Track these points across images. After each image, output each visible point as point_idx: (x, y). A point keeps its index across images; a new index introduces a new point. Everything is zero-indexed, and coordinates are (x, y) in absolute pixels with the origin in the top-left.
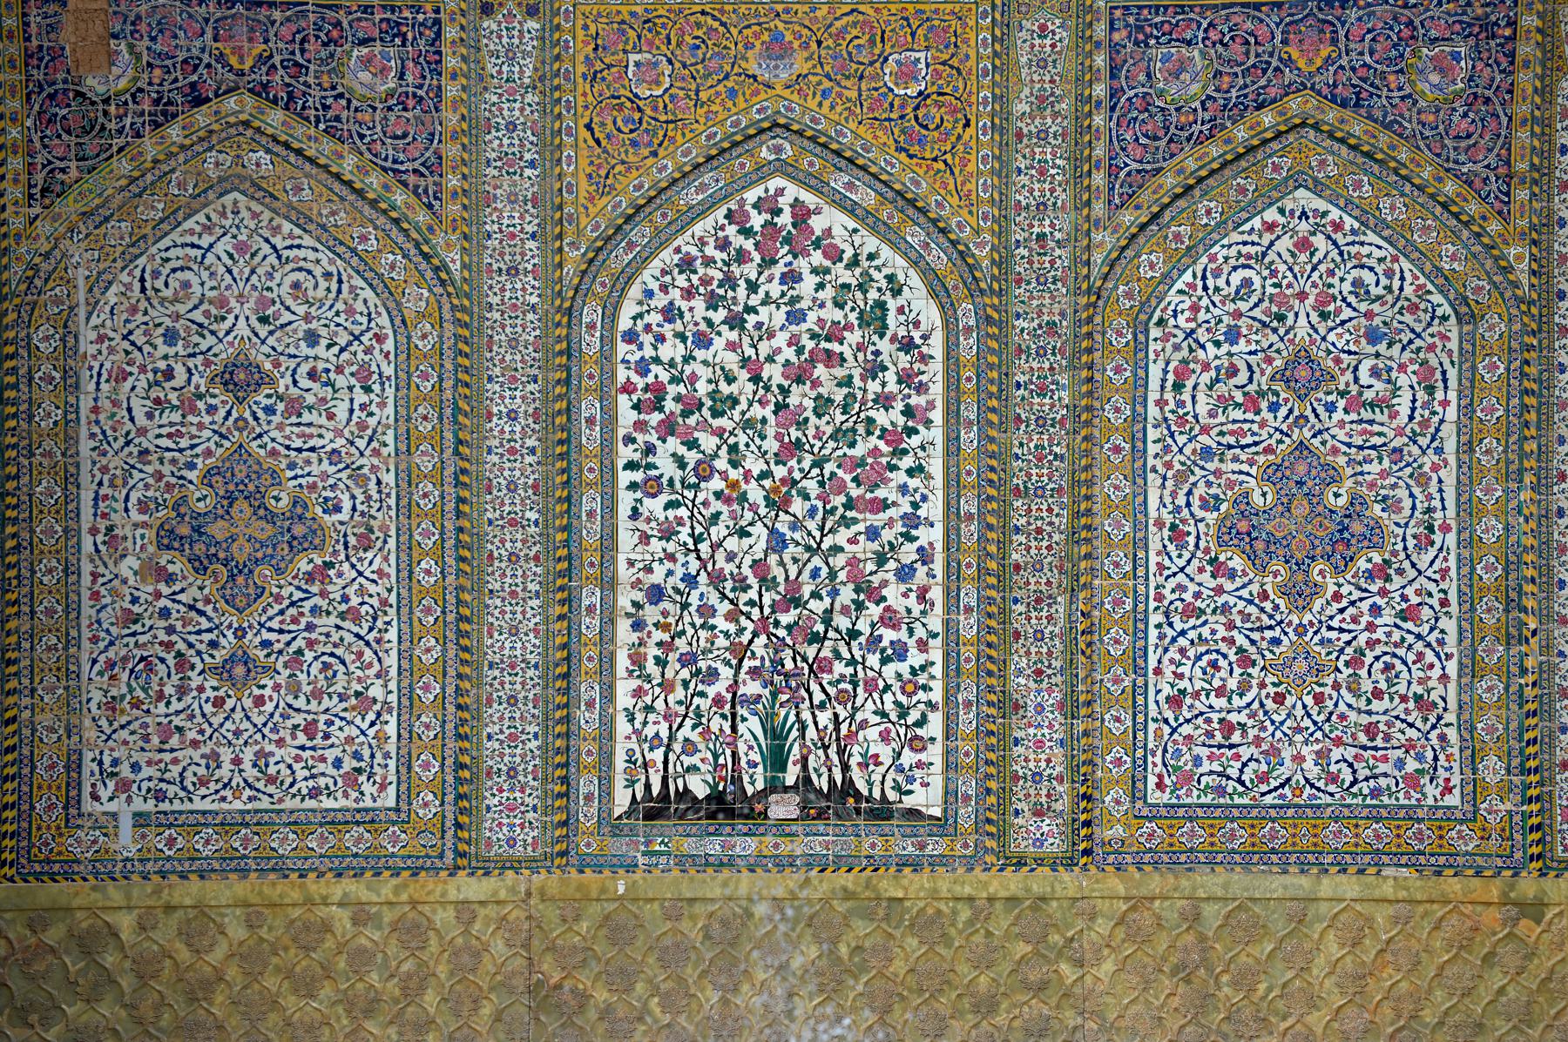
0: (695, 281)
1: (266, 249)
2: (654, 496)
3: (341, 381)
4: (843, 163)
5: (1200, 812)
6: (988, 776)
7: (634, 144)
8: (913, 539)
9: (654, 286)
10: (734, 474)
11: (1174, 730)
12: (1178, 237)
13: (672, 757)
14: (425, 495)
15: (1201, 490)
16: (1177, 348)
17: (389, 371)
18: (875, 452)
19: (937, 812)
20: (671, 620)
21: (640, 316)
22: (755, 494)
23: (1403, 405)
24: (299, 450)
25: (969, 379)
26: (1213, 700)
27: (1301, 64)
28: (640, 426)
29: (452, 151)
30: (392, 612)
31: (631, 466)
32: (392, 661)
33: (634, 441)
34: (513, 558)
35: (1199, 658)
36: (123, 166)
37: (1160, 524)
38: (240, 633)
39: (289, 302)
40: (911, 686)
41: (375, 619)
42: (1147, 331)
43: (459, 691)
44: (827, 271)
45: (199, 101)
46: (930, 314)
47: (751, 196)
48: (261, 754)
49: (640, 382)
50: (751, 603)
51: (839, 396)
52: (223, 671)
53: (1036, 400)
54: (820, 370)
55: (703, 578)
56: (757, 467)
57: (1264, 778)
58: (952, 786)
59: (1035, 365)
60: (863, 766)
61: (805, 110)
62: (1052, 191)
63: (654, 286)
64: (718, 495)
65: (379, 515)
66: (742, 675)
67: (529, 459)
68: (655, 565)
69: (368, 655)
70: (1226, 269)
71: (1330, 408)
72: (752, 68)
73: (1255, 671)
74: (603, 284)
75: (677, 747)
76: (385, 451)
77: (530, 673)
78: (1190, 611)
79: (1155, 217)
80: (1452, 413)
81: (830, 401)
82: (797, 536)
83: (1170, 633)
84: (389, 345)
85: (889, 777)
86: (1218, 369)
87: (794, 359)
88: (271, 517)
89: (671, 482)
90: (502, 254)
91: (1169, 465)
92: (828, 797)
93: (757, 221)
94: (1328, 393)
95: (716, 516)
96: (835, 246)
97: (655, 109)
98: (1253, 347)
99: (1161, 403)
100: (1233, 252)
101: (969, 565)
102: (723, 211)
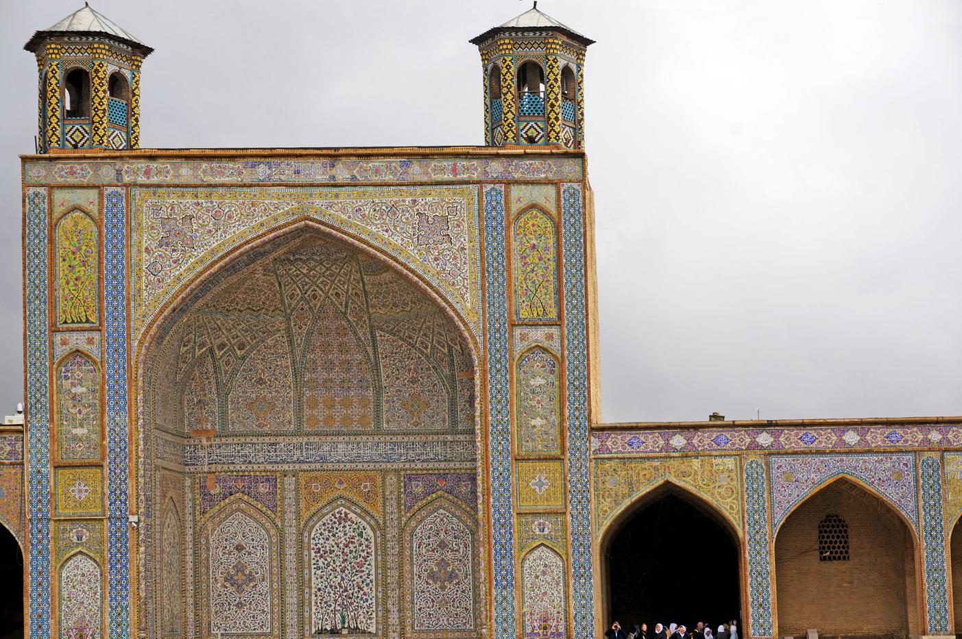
3: (258, 548)
10: (334, 566)
18: (361, 561)
22: (338, 569)
23: (461, 551)
28: (316, 556)
29: (279, 503)
31: (314, 564)
32: (269, 603)
36: (217, 507)
37: (416, 575)
38: (240, 598)
40: (369, 607)
43: (282, 609)
45: (231, 494)
46: (371, 534)
47: (336, 511)
48: (244, 622)
51: (354, 550)
52: (237, 605)
56: (338, 564)
57: (437, 624)
61: (346, 494)
63: (318, 529)
69: (264, 602)
71: (448, 552)
72: (336, 486)
75: (324, 620)
78: (422, 592)
79: (414, 515)
80: (470, 552)
84: (267, 541)
88: (245, 575)
93: (338, 516)
99: (416, 551)
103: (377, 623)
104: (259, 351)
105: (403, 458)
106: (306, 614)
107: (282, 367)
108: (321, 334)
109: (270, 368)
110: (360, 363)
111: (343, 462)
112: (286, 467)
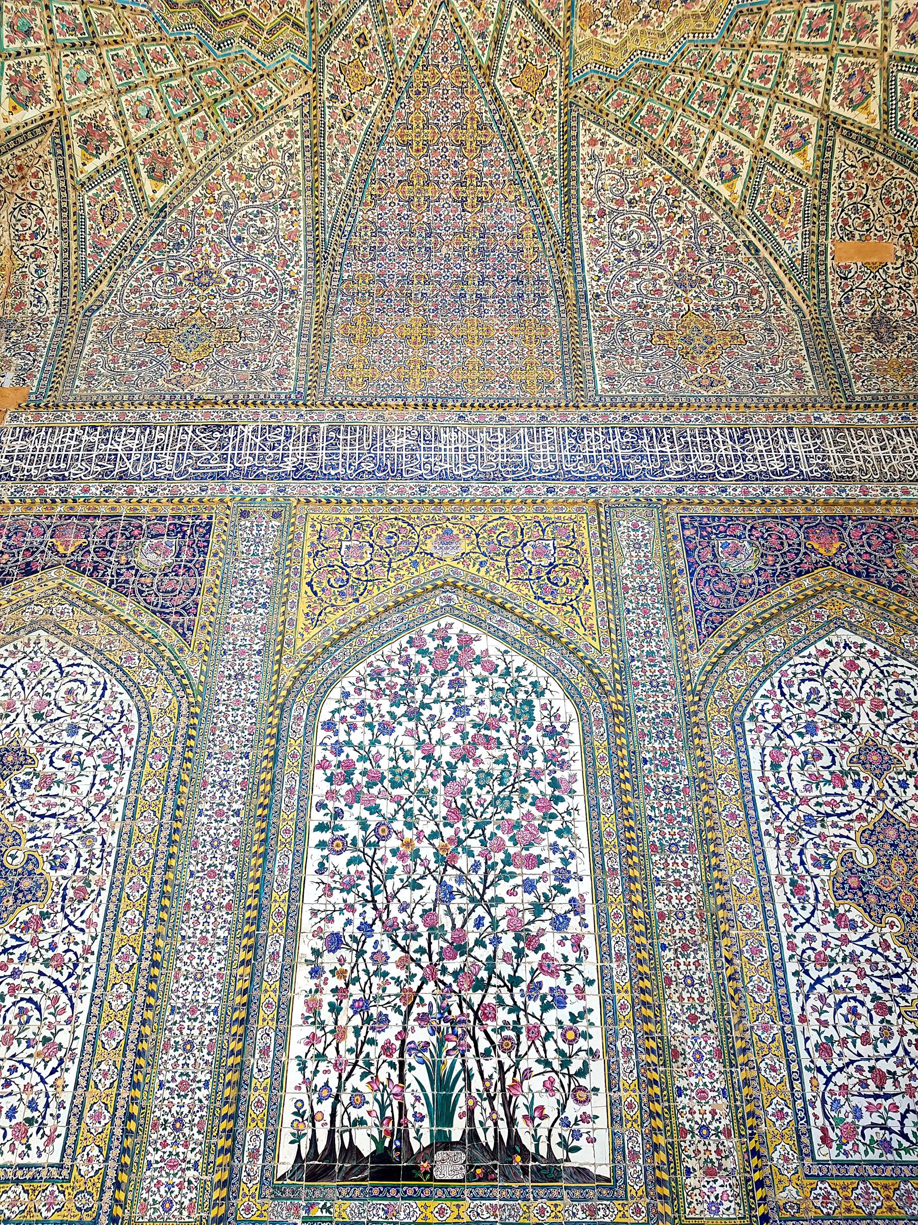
0: (382, 684)
1: (53, 666)
2: (339, 853)
3: (89, 762)
4: (496, 608)
5: (870, 1170)
6: (654, 1130)
7: (342, 594)
8: (566, 892)
9: (351, 689)
11: (829, 1080)
12: (754, 658)
13: (340, 1109)
14: (141, 854)
15: (810, 851)
16: (769, 737)
17: (129, 753)
19: (605, 1172)
20: (347, 967)
21: (338, 710)
22: (427, 852)
24: (42, 816)
25: (603, 758)
26: (860, 1048)
27: (822, 551)
28: (331, 795)
30: (92, 959)
31: (321, 827)
32: (83, 1007)
33: (325, 806)
34: (208, 907)
35: (839, 1005)
37: (781, 880)
39: (62, 704)
40: (573, 1031)
41: (76, 966)
42: (742, 724)
43: (141, 1037)
44: (485, 679)
46: (567, 709)
47: (428, 628)
49: (333, 760)
50: (421, 950)
51: (497, 770)
53: (661, 773)
54: (481, 751)
55: (378, 927)
56: (428, 828)
58: (618, 1142)
59: (657, 745)
60: (529, 1118)
62: (655, 624)
63: (351, 689)
64: (394, 852)
65: (98, 871)
66: (411, 1023)
67: (233, 820)
68: (336, 915)
70: (796, 681)
72: (429, 548)
73: (893, 1018)
74: (311, 688)
75: (345, 1098)
76: (114, 817)
77: (209, 1018)
78: (823, 960)
79: (735, 644)
81: (489, 774)
82: (463, 888)
83: (808, 981)
84: (134, 734)
85: (555, 1133)
86: (805, 754)
87: (460, 742)
89: (354, 840)
90: (233, 666)
91: (779, 830)
92: (493, 1155)
93: (431, 645)
94: (899, 773)
95: (392, 870)
96: (491, 662)
97: (359, 573)
98: (830, 738)
100: (799, 669)
101: (617, 916)
102: (407, 638)
103: (614, 1119)
104: (209, 188)
105: (673, 468)
106: (255, 1061)
107: (277, 237)
108: (409, 144)
109: (239, 239)
110: (519, 236)
111: (455, 478)
112: (250, 488)
